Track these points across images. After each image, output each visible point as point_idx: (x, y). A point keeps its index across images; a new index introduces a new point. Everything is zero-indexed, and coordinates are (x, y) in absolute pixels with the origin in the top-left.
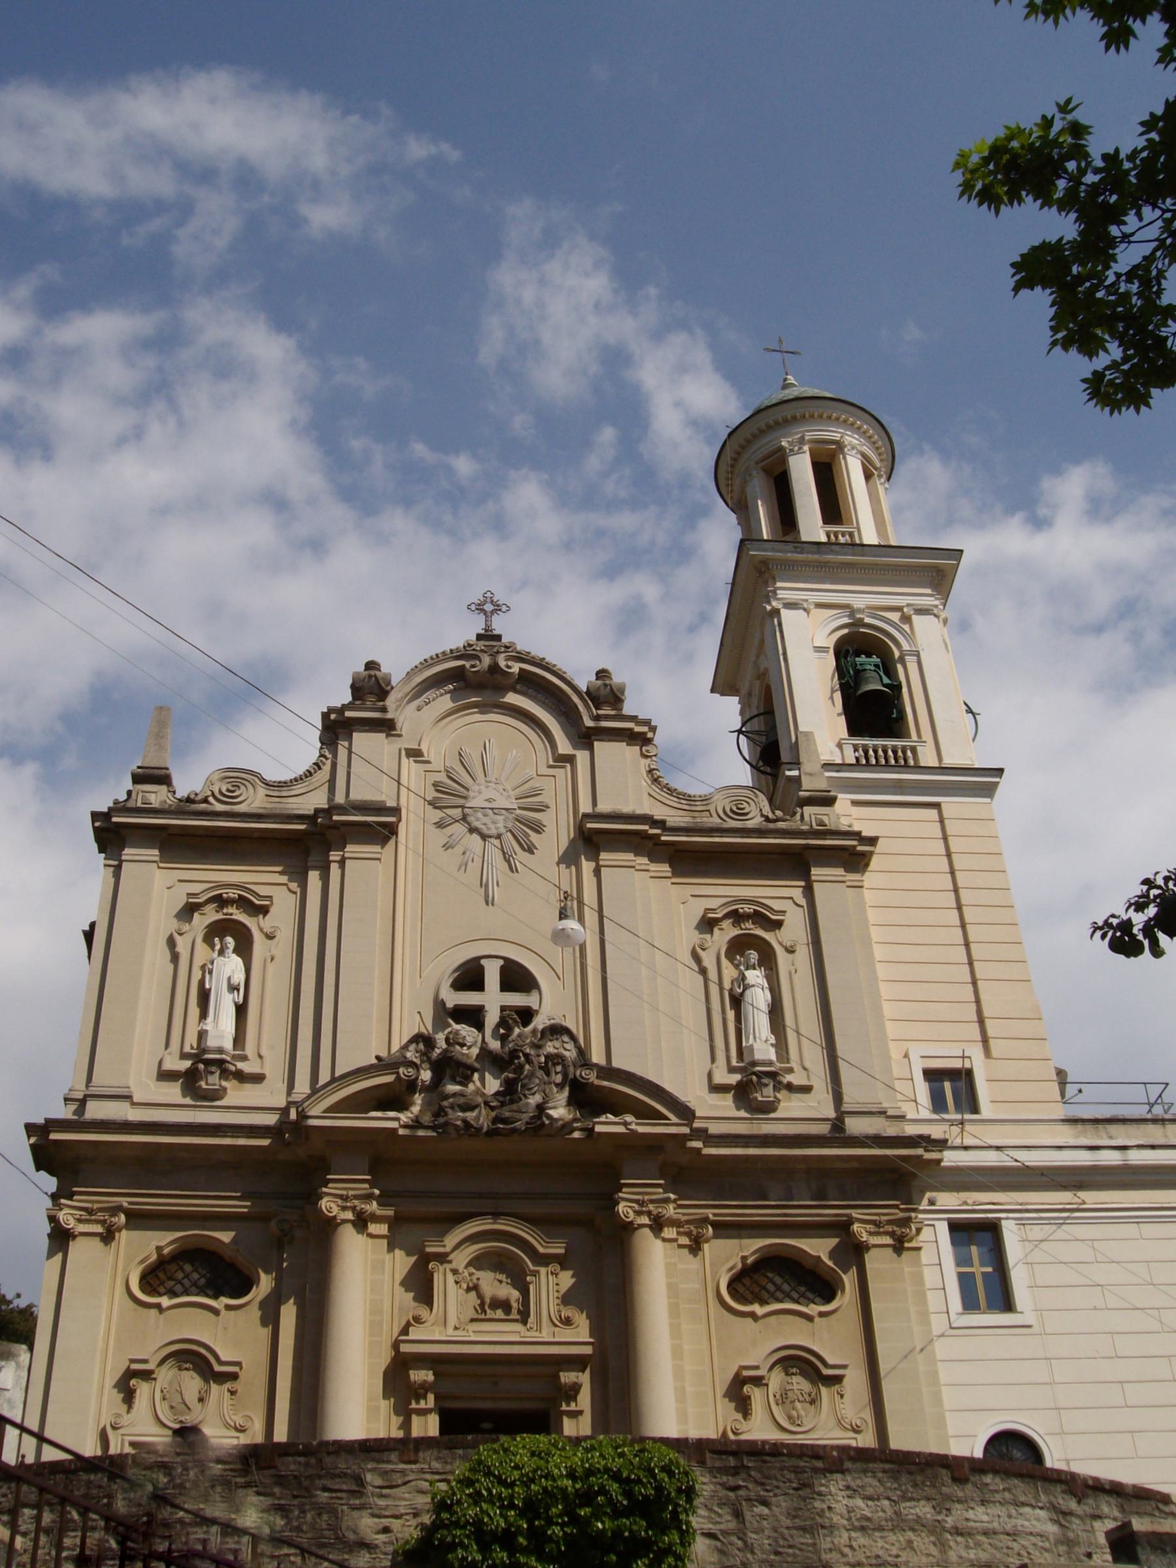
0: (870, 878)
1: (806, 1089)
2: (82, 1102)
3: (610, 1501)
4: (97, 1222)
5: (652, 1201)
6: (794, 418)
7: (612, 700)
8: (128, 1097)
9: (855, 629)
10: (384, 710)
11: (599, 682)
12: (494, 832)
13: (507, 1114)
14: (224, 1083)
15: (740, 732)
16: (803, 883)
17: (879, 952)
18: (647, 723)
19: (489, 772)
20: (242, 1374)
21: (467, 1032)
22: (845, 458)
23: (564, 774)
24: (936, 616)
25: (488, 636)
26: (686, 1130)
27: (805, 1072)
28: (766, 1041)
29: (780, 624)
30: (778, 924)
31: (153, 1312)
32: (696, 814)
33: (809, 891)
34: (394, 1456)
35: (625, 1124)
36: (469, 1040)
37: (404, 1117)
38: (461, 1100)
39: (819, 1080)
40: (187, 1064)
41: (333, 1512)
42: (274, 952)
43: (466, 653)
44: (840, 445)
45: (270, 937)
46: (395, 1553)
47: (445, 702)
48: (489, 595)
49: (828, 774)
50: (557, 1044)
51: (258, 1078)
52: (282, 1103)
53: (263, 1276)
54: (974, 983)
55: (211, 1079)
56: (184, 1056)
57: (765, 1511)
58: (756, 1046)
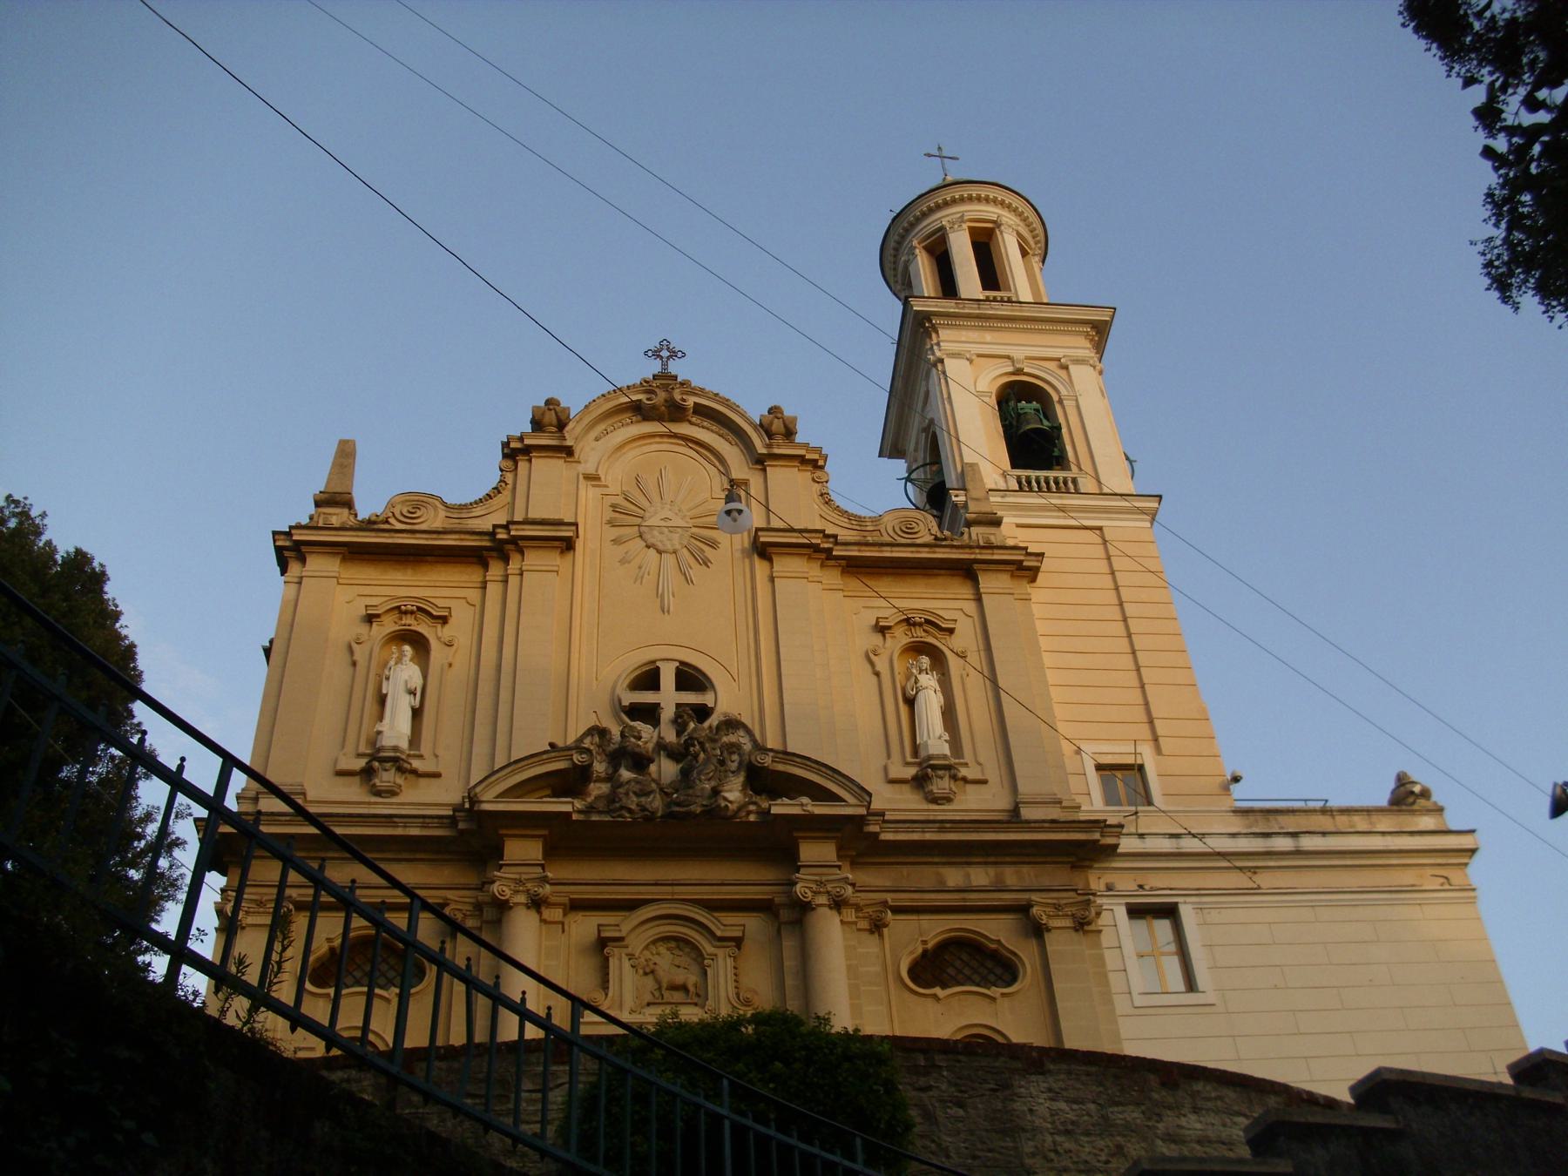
10: (564, 438)
12: (669, 547)
18: (818, 450)
19: (665, 497)
21: (645, 729)
22: (1001, 233)
26: (863, 811)
27: (979, 767)
28: (940, 737)
30: (951, 631)
32: (865, 534)
33: (978, 599)
39: (993, 772)
40: (362, 763)
44: (997, 224)
54: (1142, 686)
57: (961, 1112)
58: (929, 742)
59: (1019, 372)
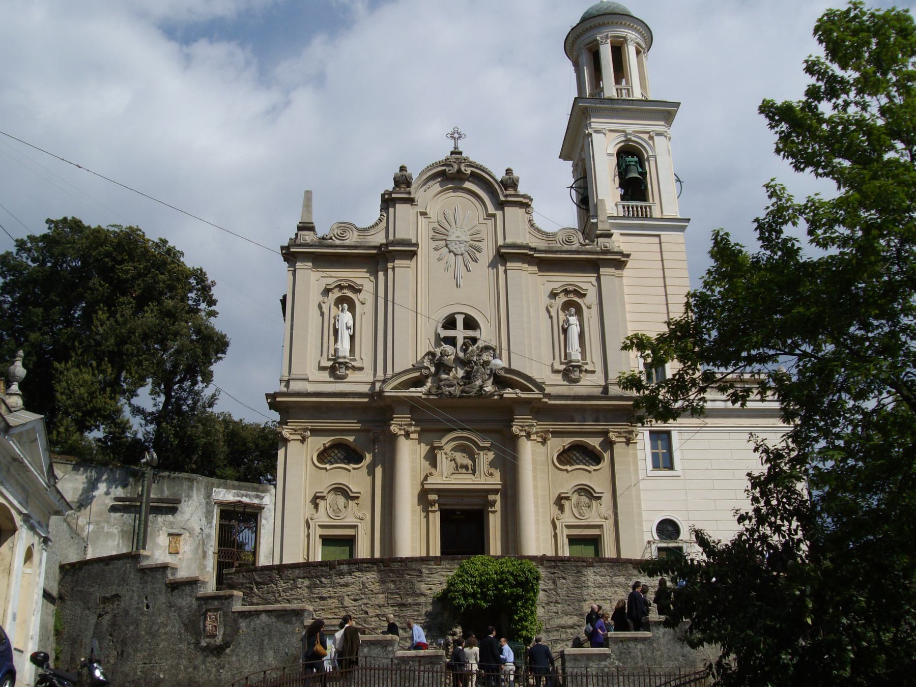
0: (626, 272)
1: (593, 372)
2: (288, 381)
3: (510, 583)
4: (298, 434)
5: (527, 426)
6: (604, 24)
7: (513, 185)
8: (307, 380)
9: (627, 143)
10: (409, 193)
11: (507, 177)
12: (460, 253)
13: (467, 389)
14: (347, 372)
15: (572, 187)
16: (596, 275)
17: (628, 307)
19: (457, 222)
20: (360, 496)
21: (449, 348)
23: (490, 222)
24: (666, 137)
25: (456, 152)
29: (592, 141)
30: (585, 295)
31: (324, 471)
33: (598, 279)
34: (432, 563)
35: (516, 393)
36: (451, 352)
37: (424, 389)
38: (448, 382)
39: (599, 368)
40: (331, 363)
41: (411, 582)
42: (365, 310)
43: (446, 163)
45: (363, 303)
46: (434, 597)
47: (436, 187)
48: (456, 129)
49: (610, 221)
50: (488, 354)
51: (361, 369)
52: (372, 380)
53: (367, 455)
55: (341, 370)
56: (329, 360)
57: (564, 581)
59: (630, 140)
